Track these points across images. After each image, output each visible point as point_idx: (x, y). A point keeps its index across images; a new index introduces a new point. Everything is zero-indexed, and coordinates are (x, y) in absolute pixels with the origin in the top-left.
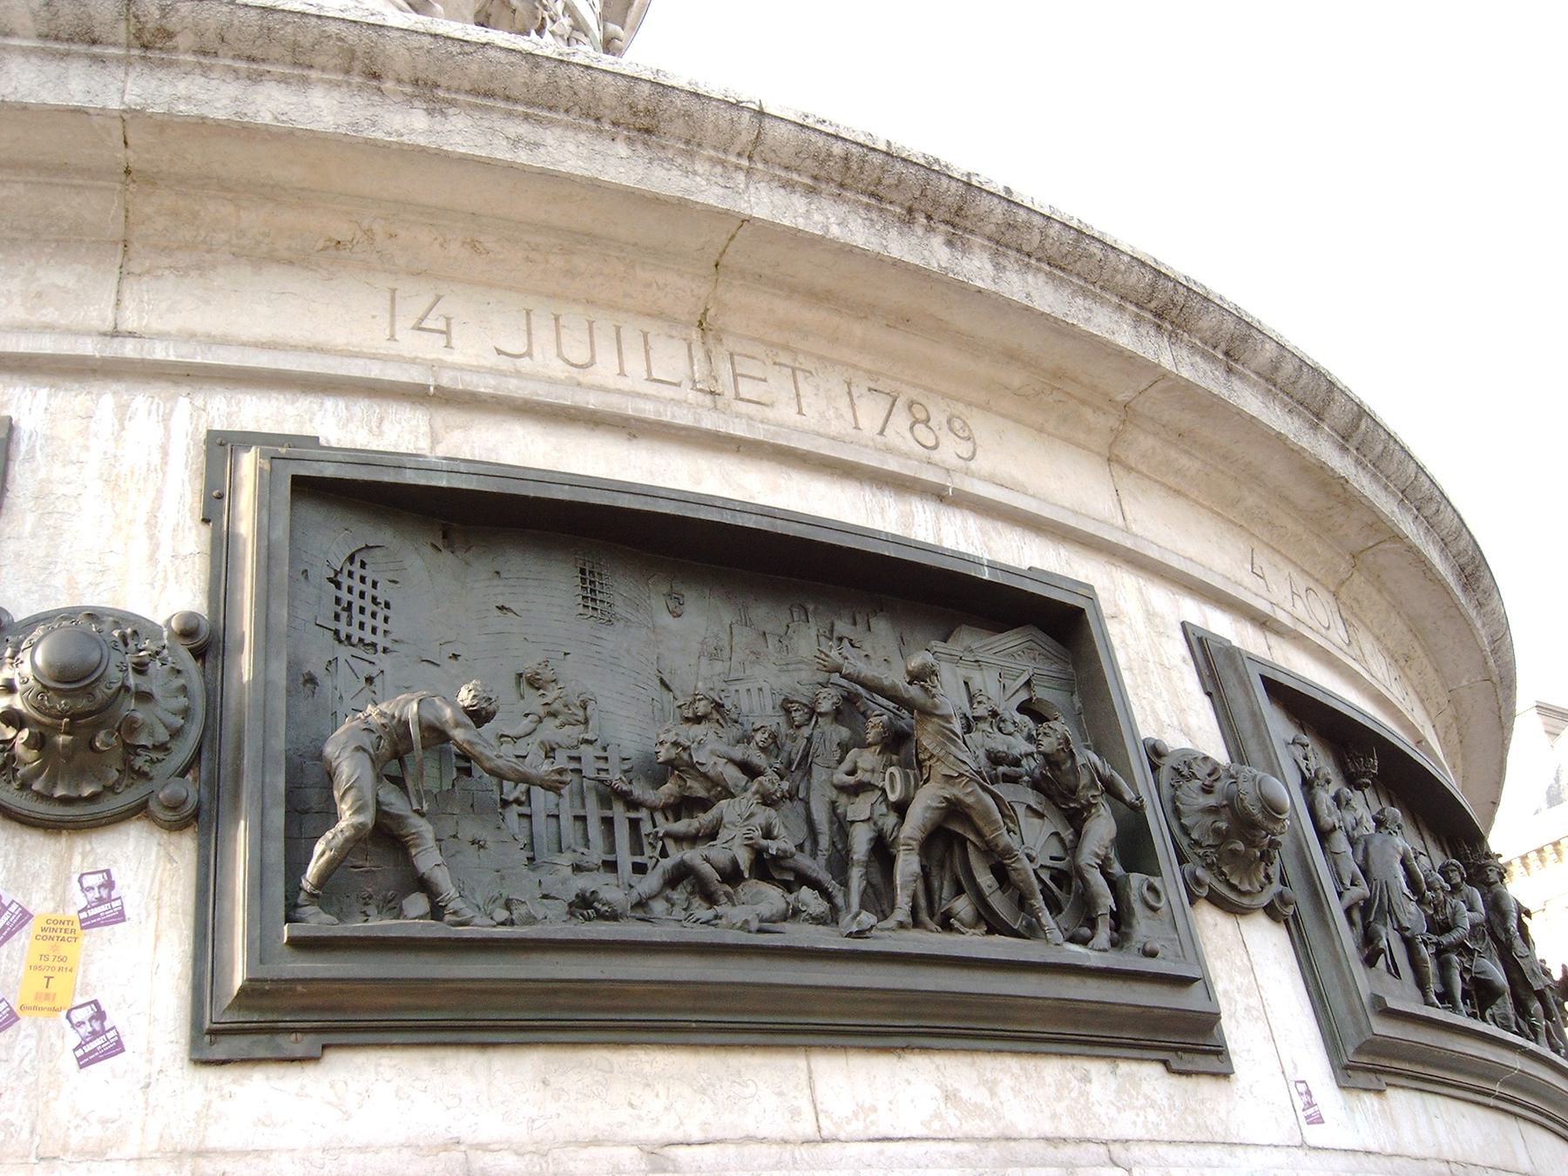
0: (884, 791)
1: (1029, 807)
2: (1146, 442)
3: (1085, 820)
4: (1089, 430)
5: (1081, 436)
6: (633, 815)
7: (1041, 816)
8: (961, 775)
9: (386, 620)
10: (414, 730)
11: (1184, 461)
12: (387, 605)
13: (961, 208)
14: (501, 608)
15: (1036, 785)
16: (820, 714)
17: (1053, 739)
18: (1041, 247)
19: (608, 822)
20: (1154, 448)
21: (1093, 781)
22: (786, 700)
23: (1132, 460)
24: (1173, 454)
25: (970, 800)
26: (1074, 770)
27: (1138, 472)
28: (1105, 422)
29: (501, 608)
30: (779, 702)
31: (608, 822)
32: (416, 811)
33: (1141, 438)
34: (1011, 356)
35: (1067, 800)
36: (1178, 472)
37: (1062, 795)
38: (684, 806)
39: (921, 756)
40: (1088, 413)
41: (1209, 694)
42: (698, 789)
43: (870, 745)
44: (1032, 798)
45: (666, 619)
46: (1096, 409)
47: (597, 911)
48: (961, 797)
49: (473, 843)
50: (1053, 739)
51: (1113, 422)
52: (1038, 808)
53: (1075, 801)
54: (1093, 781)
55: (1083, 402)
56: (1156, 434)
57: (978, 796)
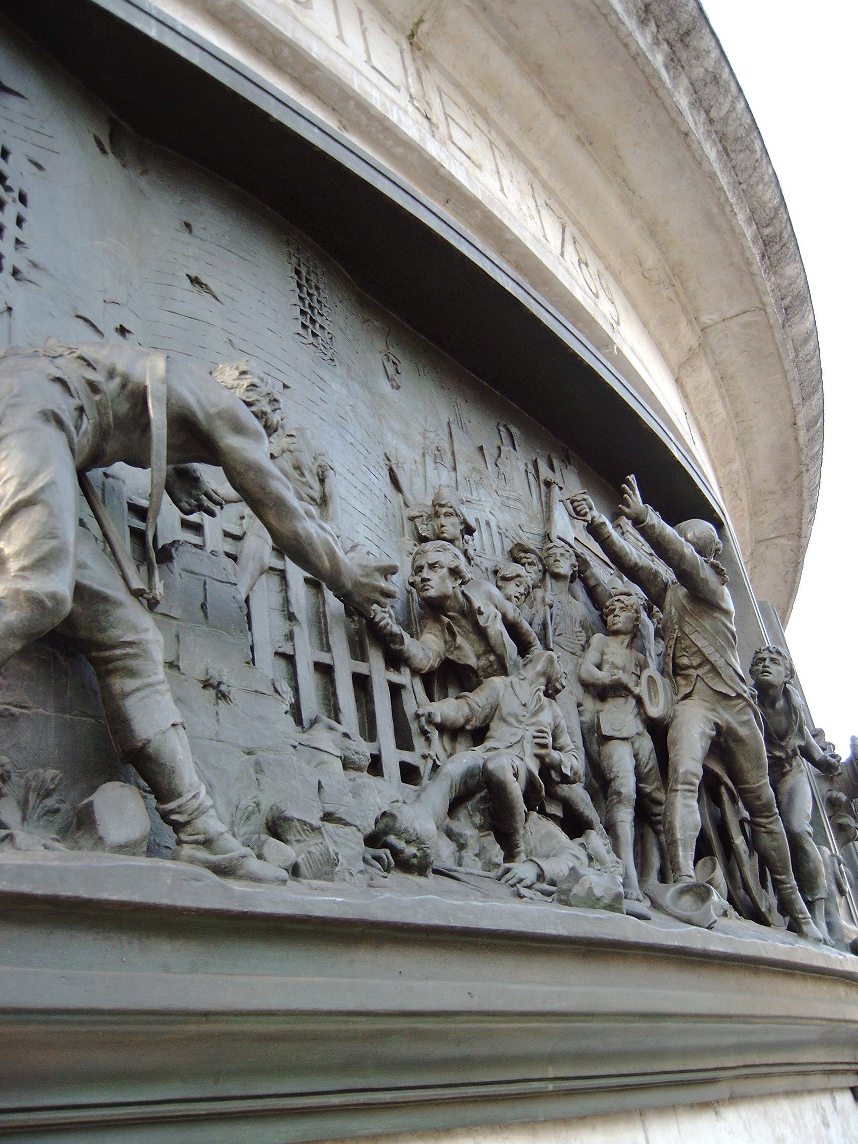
0: (639, 701)
5: (667, 346)
6: (396, 678)
8: (739, 696)
9: (20, 221)
10: (158, 415)
12: (23, 199)
13: (688, 33)
14: (195, 281)
16: (557, 576)
17: (782, 669)
18: (725, 119)
19: (362, 683)
20: (708, 383)
22: (519, 545)
23: (689, 387)
25: (743, 732)
28: (688, 337)
29: (195, 281)
30: (508, 546)
31: (362, 683)
32: (137, 594)
33: (705, 367)
34: (652, 229)
36: (709, 415)
38: (450, 677)
39: (685, 661)
42: (469, 653)
43: (616, 633)
45: (385, 387)
46: (689, 322)
47: (396, 852)
48: (734, 724)
49: (206, 685)
50: (782, 669)
51: (694, 343)
53: (783, 748)
57: (752, 728)
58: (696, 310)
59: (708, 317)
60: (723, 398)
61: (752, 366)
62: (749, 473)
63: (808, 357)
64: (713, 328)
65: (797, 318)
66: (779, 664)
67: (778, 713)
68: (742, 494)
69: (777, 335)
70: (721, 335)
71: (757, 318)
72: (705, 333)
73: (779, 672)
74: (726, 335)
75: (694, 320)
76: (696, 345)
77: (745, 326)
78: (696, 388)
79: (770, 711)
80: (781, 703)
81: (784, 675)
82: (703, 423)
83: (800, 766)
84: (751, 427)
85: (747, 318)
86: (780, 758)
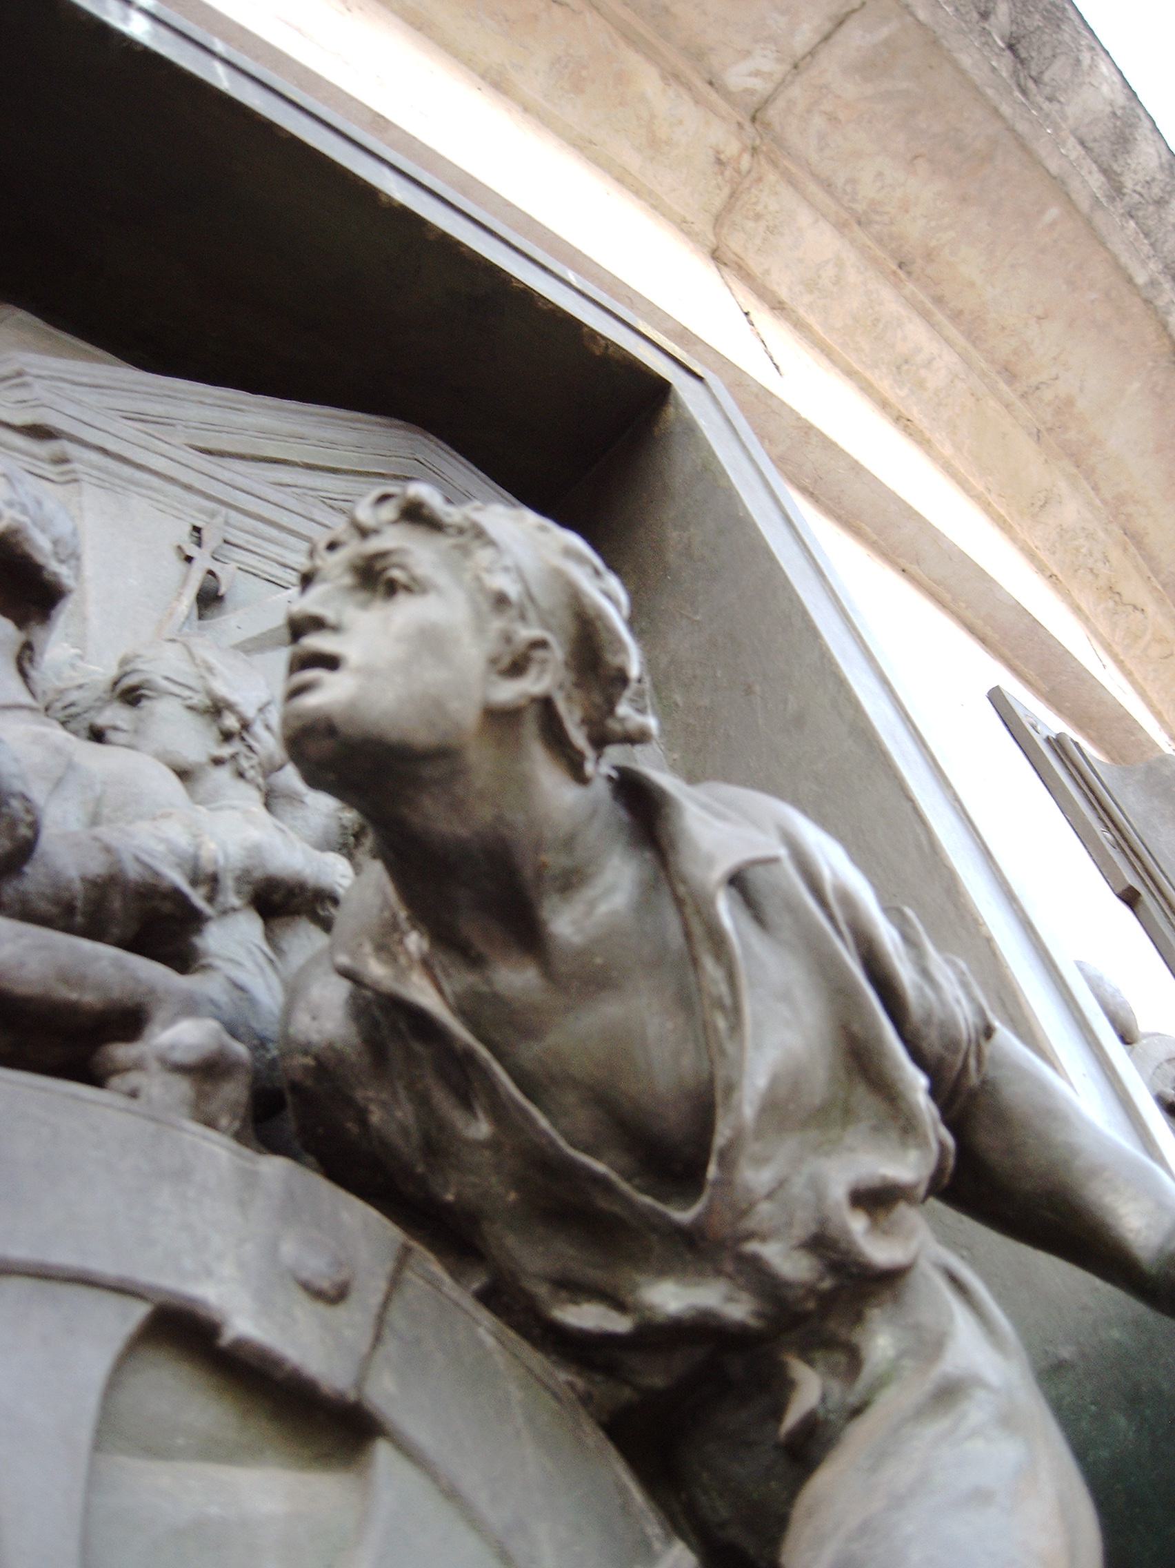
1: (179, 1330)
3: (808, 1448)
4: (654, 145)
5: (633, 161)
7: (329, 1426)
11: (916, 334)
15: (288, 1108)
20: (840, 264)
21: (860, 1059)
24: (890, 303)
26: (685, 944)
27: (799, 326)
33: (804, 217)
35: (609, 1237)
36: (902, 366)
37: (562, 1200)
40: (648, 81)
41: (1130, 898)
44: (251, 1242)
46: (672, 77)
52: (311, 1346)
53: (696, 1250)
54: (860, 1059)
55: (632, 39)
56: (841, 227)
58: (697, 55)
59: (745, 66)
60: (925, 315)
61: (964, 199)
62: (1134, 538)
63: (1156, 191)
64: (780, 103)
65: (1057, 72)
66: (414, 587)
67: (590, 978)
68: (1135, 589)
69: (966, 61)
70: (818, 122)
71: (884, 32)
72: (767, 126)
73: (430, 641)
74: (832, 118)
75: (695, 72)
76: (732, 148)
77: (871, 66)
78: (811, 285)
79: (516, 978)
80: (600, 903)
81: (472, 653)
82: (885, 385)
83: (930, 1345)
84: (1070, 402)
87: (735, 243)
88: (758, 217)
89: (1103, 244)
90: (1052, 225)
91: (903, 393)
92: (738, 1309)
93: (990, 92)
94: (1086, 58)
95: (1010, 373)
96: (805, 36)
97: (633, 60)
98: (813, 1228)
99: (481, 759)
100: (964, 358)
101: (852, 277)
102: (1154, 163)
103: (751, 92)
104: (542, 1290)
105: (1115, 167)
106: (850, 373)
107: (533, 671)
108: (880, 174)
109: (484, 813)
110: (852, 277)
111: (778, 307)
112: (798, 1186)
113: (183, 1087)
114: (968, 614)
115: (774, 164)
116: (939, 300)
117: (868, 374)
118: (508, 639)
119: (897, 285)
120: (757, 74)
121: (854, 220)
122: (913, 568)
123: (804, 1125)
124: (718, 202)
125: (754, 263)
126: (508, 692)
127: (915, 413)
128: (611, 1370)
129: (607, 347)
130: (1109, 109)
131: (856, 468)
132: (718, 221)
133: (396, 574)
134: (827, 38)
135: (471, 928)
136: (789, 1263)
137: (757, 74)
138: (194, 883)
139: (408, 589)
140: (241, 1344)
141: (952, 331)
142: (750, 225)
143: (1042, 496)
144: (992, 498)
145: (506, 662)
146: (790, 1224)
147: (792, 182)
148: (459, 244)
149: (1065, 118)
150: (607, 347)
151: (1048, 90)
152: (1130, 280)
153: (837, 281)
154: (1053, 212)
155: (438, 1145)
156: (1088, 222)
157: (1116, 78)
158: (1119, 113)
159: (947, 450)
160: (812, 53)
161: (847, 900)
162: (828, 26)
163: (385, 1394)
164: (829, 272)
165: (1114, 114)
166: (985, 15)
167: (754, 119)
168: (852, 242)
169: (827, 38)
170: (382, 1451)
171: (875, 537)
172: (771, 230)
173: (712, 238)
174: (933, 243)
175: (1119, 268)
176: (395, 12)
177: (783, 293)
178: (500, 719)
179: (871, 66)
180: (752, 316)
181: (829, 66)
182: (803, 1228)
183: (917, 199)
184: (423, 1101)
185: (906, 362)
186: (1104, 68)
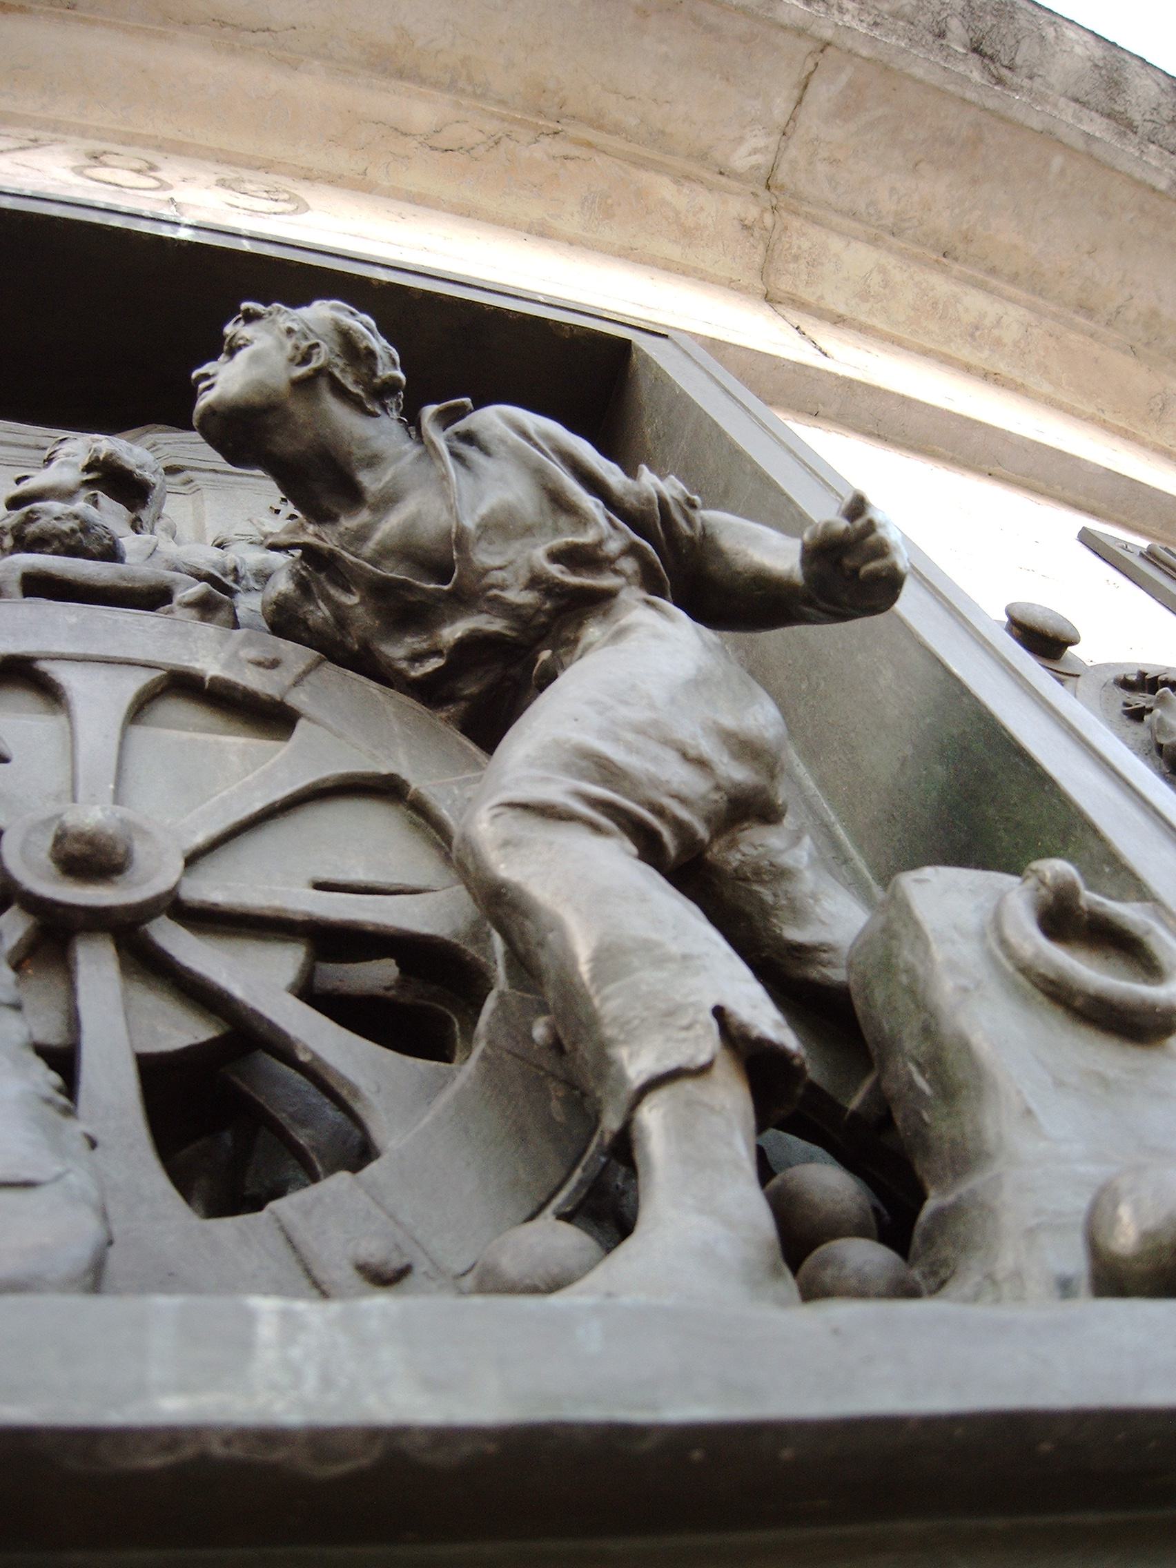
1: (182, 685)
2: (860, 258)
4: (688, 234)
5: (673, 251)
7: (272, 718)
11: (975, 303)
20: (883, 270)
23: (837, 302)
24: (941, 286)
27: (864, 330)
28: (720, 210)
36: (974, 333)
40: (664, 188)
51: (740, 207)
55: (641, 163)
56: (874, 241)
58: (703, 157)
59: (743, 150)
61: (975, 181)
64: (784, 166)
69: (919, 72)
70: (822, 168)
71: (843, 78)
72: (782, 188)
74: (833, 162)
75: (705, 168)
76: (752, 213)
77: (845, 109)
78: (864, 296)
82: (965, 353)
84: (1154, 314)
85: (823, 93)
86: (473, 645)
87: (784, 285)
88: (796, 258)
89: (1113, 169)
90: (1063, 172)
91: (986, 353)
92: (494, 625)
93: (951, 88)
94: (1050, 33)
95: (1086, 309)
96: (780, 108)
97: (646, 178)
98: (528, 575)
99: (299, 409)
100: (1031, 308)
101: (897, 276)
102: (1154, 91)
103: (757, 167)
104: (403, 665)
105: (1117, 108)
106: (925, 353)
107: (314, 358)
108: (893, 190)
109: (309, 434)
110: (897, 276)
111: (838, 321)
112: (520, 561)
113: (192, 612)
114: (1068, 494)
115: (796, 213)
116: (993, 271)
117: (944, 349)
118: (297, 348)
119: (945, 271)
120: (755, 151)
121: (885, 232)
122: (996, 469)
123: (523, 535)
124: (758, 259)
125: (807, 294)
126: (300, 371)
127: (1002, 367)
128: (451, 699)
129: (572, 330)
130: (1089, 64)
131: (905, 401)
132: (763, 273)
133: (241, 342)
134: (799, 102)
135: (327, 503)
136: (518, 596)
137: (755, 151)
138: (225, 575)
139: (245, 345)
140: (214, 680)
141: (1011, 290)
142: (792, 266)
143: (1158, 399)
144: (1107, 416)
145: (299, 358)
146: (517, 580)
147: (815, 221)
148: (438, 294)
149: (1050, 86)
150: (572, 330)
151: (1025, 71)
152: (1154, 190)
153: (886, 284)
154: (1057, 161)
155: (341, 617)
156: (1090, 156)
157: (1088, 37)
158: (1101, 64)
159: (1047, 388)
160: (793, 118)
161: (547, 437)
162: (796, 93)
163: (298, 699)
164: (876, 278)
165: (1096, 66)
166: (942, 35)
167: (768, 187)
168: (890, 250)
169: (799, 102)
170: (301, 723)
171: (951, 454)
172: (812, 264)
173: (760, 286)
174: (965, 227)
175: (1139, 183)
176: (444, 211)
177: (841, 309)
178: (300, 385)
179: (845, 109)
180: (802, 329)
181: (811, 123)
182: (524, 576)
183: (935, 196)
184: (328, 599)
185: (977, 328)
186: (1071, 33)
